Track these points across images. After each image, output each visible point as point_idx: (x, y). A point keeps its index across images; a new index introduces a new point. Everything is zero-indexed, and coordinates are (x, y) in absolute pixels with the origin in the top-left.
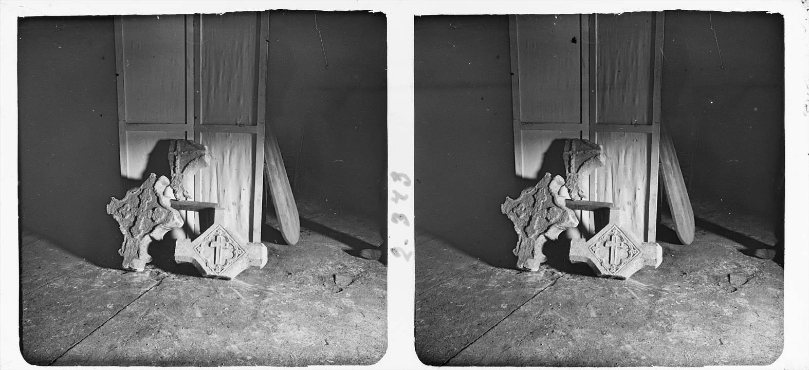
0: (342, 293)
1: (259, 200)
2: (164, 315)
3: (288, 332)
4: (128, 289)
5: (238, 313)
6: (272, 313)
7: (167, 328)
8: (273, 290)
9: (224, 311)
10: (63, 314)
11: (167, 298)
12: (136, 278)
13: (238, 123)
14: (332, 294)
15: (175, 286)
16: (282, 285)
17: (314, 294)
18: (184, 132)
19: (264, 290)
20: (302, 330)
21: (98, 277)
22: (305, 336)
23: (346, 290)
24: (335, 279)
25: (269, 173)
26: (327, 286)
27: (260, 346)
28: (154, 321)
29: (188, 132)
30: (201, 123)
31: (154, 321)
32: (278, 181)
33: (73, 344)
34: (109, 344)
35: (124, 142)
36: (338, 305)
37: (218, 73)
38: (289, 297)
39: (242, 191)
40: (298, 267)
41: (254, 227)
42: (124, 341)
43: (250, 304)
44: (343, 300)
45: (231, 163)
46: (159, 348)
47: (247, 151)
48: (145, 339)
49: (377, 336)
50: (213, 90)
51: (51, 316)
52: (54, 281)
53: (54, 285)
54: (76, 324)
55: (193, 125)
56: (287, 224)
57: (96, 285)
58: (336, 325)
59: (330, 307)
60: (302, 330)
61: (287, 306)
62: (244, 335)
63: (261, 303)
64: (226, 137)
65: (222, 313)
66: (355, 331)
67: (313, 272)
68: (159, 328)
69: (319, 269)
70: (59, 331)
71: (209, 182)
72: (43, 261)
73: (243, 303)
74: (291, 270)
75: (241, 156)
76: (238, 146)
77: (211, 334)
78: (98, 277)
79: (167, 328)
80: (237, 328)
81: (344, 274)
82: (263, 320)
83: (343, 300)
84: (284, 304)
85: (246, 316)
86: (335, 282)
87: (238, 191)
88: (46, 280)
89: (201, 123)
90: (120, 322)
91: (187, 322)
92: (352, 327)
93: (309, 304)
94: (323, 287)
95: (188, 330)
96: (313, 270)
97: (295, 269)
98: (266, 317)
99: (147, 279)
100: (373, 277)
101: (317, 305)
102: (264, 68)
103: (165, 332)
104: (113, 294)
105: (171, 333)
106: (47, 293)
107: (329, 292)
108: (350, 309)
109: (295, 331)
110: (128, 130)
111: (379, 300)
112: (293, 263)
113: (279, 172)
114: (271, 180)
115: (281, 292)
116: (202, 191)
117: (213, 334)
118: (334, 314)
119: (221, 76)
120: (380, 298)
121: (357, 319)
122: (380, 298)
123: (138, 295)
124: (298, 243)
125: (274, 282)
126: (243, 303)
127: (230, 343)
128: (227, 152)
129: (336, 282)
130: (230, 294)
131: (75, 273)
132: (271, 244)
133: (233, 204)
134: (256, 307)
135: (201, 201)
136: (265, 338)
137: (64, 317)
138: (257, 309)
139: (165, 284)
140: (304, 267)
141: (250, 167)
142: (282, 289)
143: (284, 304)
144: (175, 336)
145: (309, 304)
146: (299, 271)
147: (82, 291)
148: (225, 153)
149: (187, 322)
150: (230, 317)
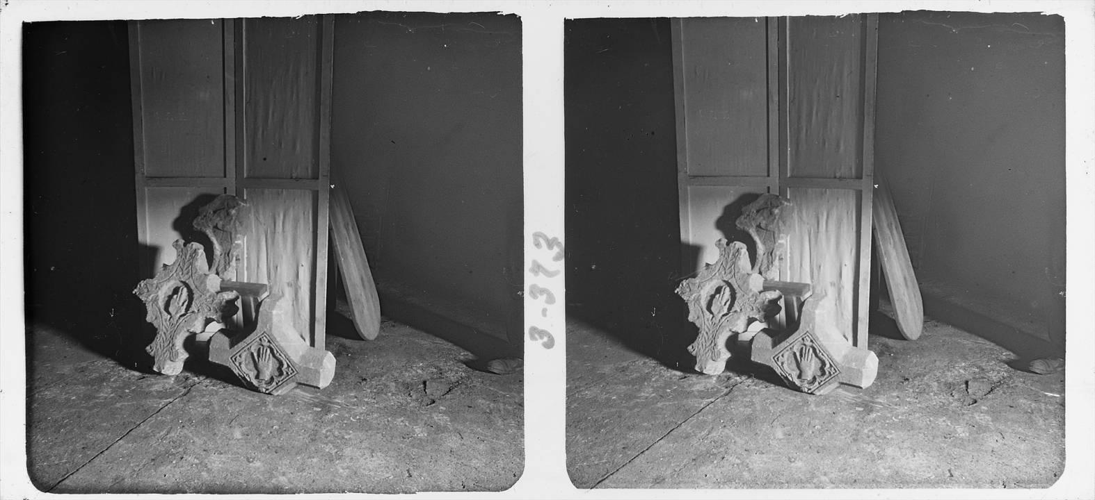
0: (976, 406)
1: (865, 280)
2: (732, 435)
3: (899, 459)
4: (685, 400)
5: (833, 433)
6: (878, 433)
7: (736, 453)
8: (882, 401)
9: (814, 430)
10: (595, 434)
11: (737, 412)
12: (698, 385)
13: (838, 175)
14: (962, 407)
15: (750, 396)
16: (895, 394)
17: (938, 407)
18: (766, 188)
19: (871, 402)
20: (919, 456)
21: (646, 384)
22: (921, 464)
23: (982, 401)
24: (967, 387)
25: (881, 243)
26: (956, 397)
27: (859, 477)
28: (718, 444)
29: (771, 188)
30: (789, 175)
31: (718, 444)
32: (893, 253)
33: (605, 475)
34: (654, 475)
35: (686, 201)
36: (970, 422)
37: (810, 115)
38: (903, 411)
39: (843, 267)
40: (918, 371)
41: (859, 316)
42: (675, 471)
43: (850, 420)
44: (976, 415)
45: (828, 229)
46: (723, 480)
47: (849, 213)
48: (703, 468)
49: (1019, 465)
50: (804, 131)
51: (578, 437)
52: (587, 388)
53: (587, 394)
54: (611, 447)
55: (778, 178)
56: (905, 312)
57: (643, 394)
58: (965, 450)
59: (958, 425)
60: (919, 456)
61: (901, 424)
62: (839, 462)
63: (865, 419)
64: (822, 194)
65: (811, 433)
66: (991, 458)
67: (938, 377)
68: (723, 453)
69: (946, 373)
70: (587, 458)
71: (799, 257)
72: (573, 361)
73: (840, 419)
74: (909, 374)
75: (842, 220)
76: (837, 206)
77: (794, 462)
78: (646, 384)
79: (736, 453)
80: (830, 453)
81: (981, 380)
82: (867, 443)
83: (976, 415)
84: (896, 420)
85: (843, 437)
86: (967, 390)
87: (838, 265)
88: (576, 388)
89: (789, 175)
90: (671, 445)
91: (762, 445)
92: (986, 452)
93: (930, 421)
94: (951, 398)
95: (764, 456)
96: (938, 374)
97: (914, 374)
98: (871, 438)
99: (713, 386)
100: (1020, 384)
101: (942, 422)
102: (872, 102)
103: (732, 459)
104: (664, 407)
105: (740, 460)
106: (575, 405)
107: (959, 404)
108: (985, 427)
109: (908, 458)
110: (690, 185)
111: (1026, 416)
112: (912, 364)
113: (894, 241)
114: (883, 252)
115: (893, 404)
116: (790, 267)
117: (796, 462)
118: (964, 435)
119: (814, 112)
120: (1027, 412)
121: (992, 441)
122: (1027, 412)
123: (699, 407)
124: (920, 338)
125: (884, 390)
126: (840, 419)
127: (819, 475)
128: (822, 215)
129: (969, 390)
130: (824, 407)
131: (616, 378)
132: (884, 339)
133: (831, 283)
134: (858, 425)
135: (788, 281)
136: (868, 467)
137: (596, 438)
138: (858, 428)
139: (736, 393)
140: (927, 370)
141: (854, 235)
142: (894, 400)
143: (896, 420)
144: (745, 464)
145: (930, 421)
146: (919, 375)
147: (624, 402)
148: (820, 216)
149: (762, 445)
150: (822, 439)
